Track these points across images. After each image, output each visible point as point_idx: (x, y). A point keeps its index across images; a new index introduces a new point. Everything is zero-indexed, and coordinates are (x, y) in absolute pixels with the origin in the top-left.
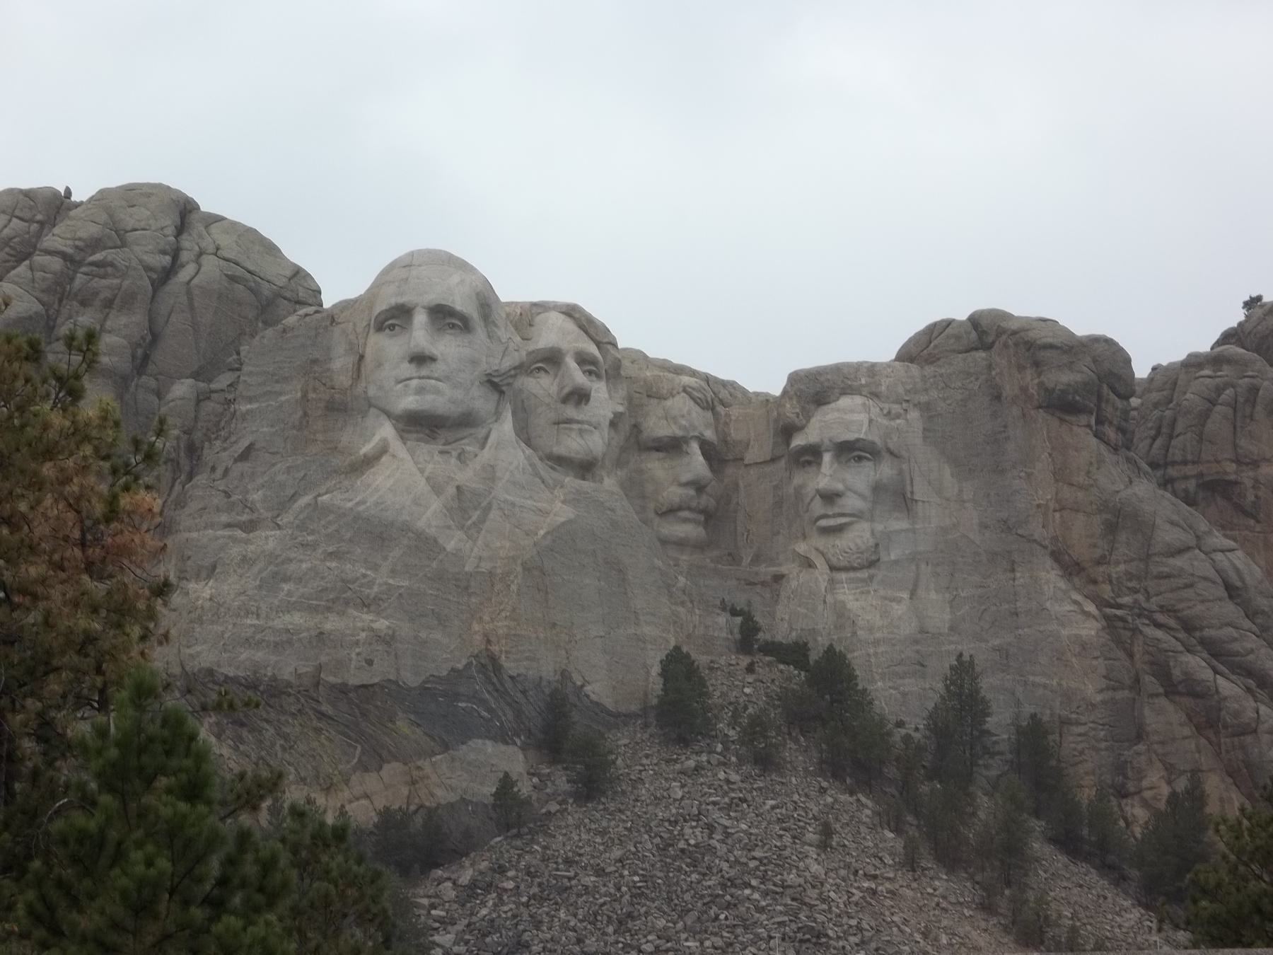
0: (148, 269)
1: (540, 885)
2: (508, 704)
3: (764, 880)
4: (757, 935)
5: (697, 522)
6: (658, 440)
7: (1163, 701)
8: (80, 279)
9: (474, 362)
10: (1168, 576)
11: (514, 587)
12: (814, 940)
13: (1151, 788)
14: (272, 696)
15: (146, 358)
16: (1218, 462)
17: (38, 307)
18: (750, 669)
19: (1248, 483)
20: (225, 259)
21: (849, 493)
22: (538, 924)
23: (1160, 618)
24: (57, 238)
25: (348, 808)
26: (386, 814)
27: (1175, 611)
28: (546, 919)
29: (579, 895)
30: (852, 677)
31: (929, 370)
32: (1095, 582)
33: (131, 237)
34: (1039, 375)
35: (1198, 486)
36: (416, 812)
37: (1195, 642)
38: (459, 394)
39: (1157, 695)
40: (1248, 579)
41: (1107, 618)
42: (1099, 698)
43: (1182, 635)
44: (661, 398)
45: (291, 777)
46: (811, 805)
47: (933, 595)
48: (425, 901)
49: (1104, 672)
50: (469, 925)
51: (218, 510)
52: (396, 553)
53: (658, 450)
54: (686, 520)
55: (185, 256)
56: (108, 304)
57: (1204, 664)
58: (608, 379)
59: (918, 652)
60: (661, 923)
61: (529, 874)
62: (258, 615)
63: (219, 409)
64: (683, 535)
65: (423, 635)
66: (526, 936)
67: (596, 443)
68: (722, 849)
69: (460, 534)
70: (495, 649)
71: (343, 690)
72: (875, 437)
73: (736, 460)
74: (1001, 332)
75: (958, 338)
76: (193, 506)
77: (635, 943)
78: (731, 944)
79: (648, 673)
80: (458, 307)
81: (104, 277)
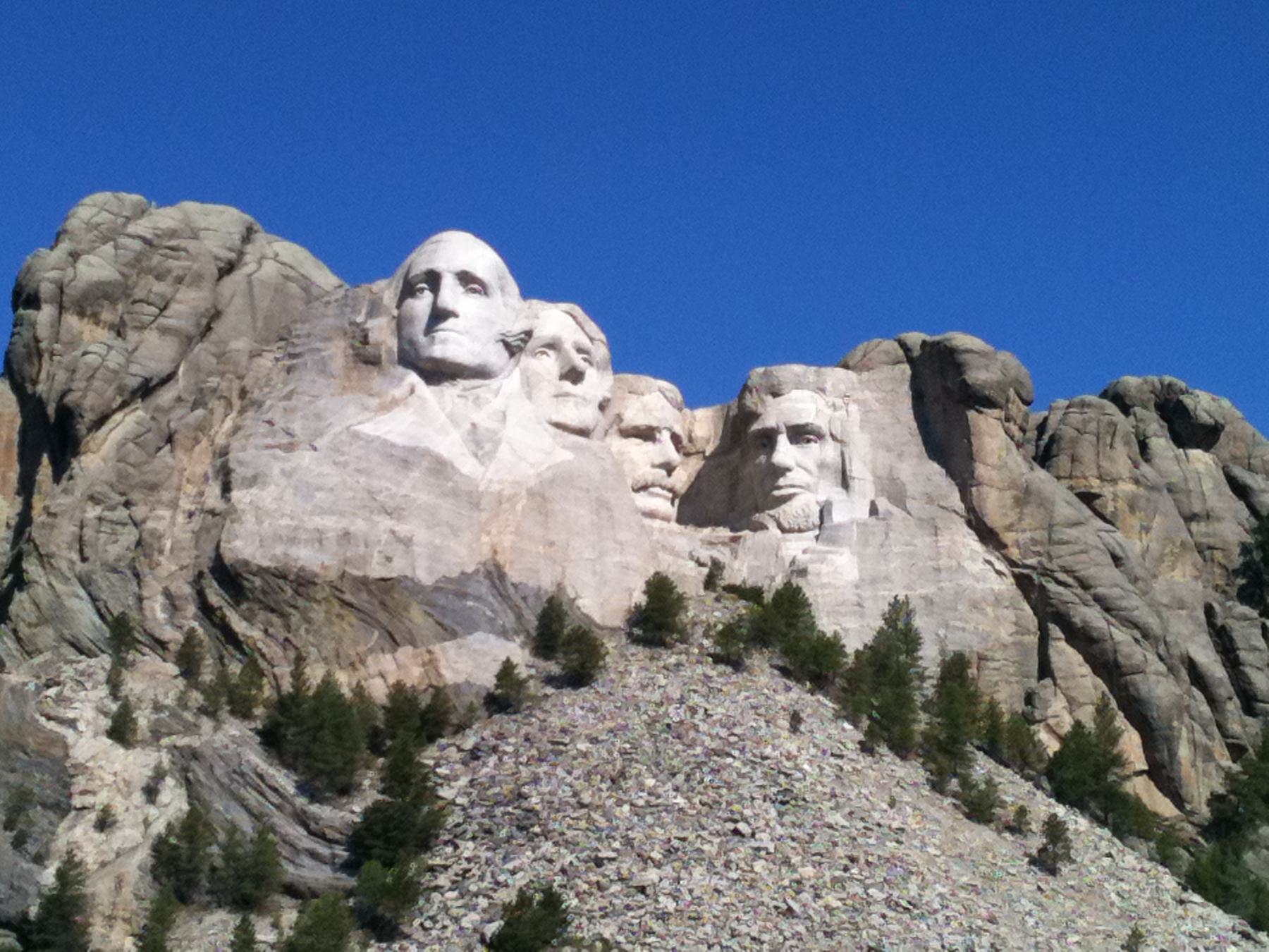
0: (217, 258)
1: (538, 749)
2: (511, 608)
3: (742, 751)
4: (742, 798)
5: (666, 498)
6: (636, 428)
7: (1063, 645)
8: (156, 260)
9: (492, 323)
10: (1067, 543)
11: (519, 507)
12: (793, 802)
13: (1056, 716)
14: (300, 585)
15: (208, 328)
16: (1086, 478)
17: (118, 276)
18: (717, 600)
19: (1110, 497)
20: (283, 264)
21: (796, 469)
22: (536, 780)
23: (1062, 576)
24: (142, 227)
25: (363, 683)
26: (398, 688)
27: (1073, 572)
28: (542, 775)
29: (575, 758)
30: (805, 604)
31: (865, 375)
32: (1005, 546)
33: (202, 234)
34: (961, 373)
36: (425, 690)
37: (1089, 597)
38: (477, 347)
39: (1059, 639)
40: (1130, 554)
41: (1015, 576)
42: (1010, 640)
43: (1079, 591)
45: (312, 657)
46: (778, 697)
47: (870, 550)
48: (431, 763)
49: (1014, 619)
50: (471, 781)
51: (265, 436)
52: (416, 474)
53: (636, 436)
54: (658, 495)
55: (248, 258)
56: (180, 280)
57: (1099, 615)
58: (598, 369)
59: (859, 596)
60: (650, 782)
61: (527, 739)
62: (292, 518)
63: (270, 364)
64: (654, 508)
65: (437, 541)
66: (525, 790)
68: (703, 727)
69: (474, 460)
70: (501, 559)
71: (364, 582)
73: (698, 453)
74: (924, 343)
75: (887, 353)
76: (240, 433)
77: (626, 798)
78: (716, 802)
79: (631, 595)
81: (177, 259)
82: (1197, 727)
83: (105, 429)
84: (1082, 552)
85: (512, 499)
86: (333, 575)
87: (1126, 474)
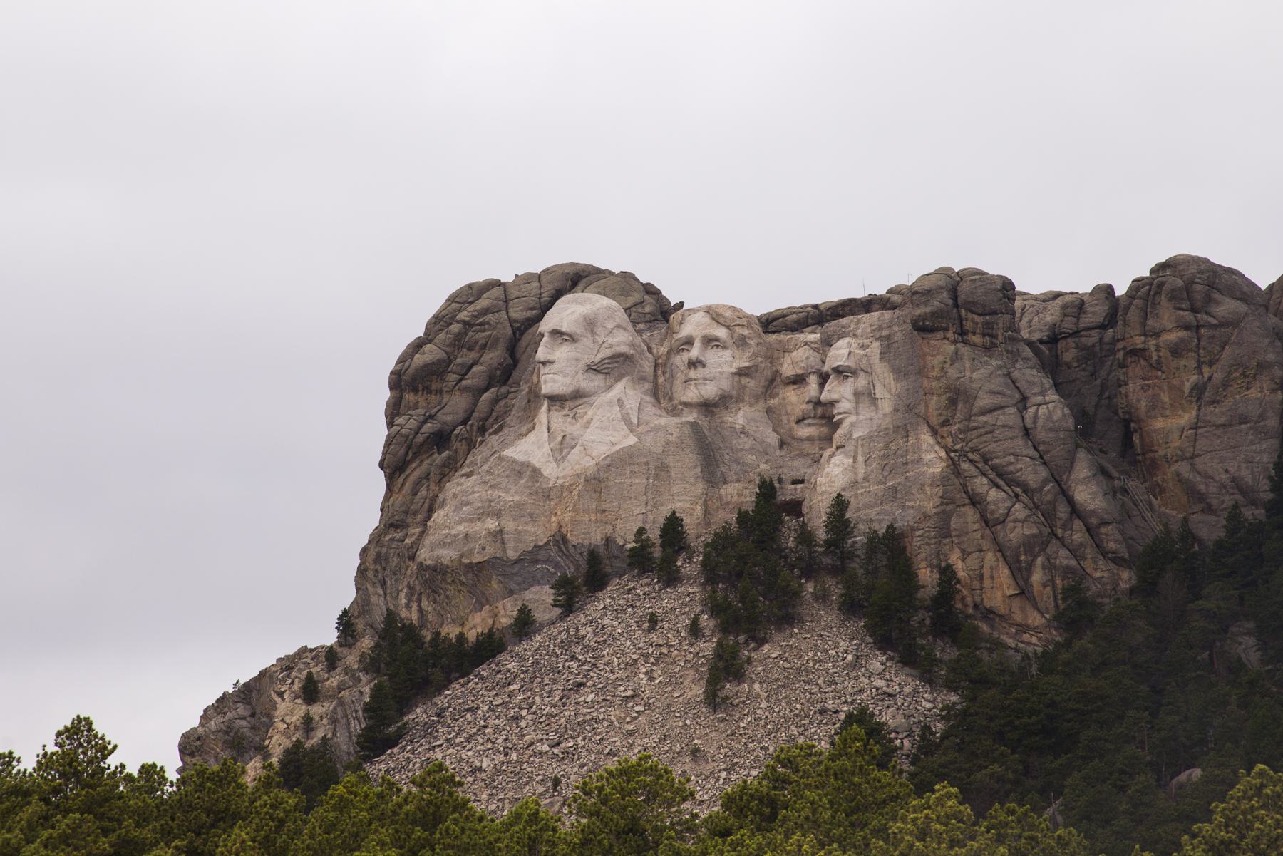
5: (822, 425)
11: (576, 492)
19: (1153, 348)
35: (1125, 355)
38: (567, 380)
39: (964, 505)
42: (934, 511)
44: (790, 352)
53: (794, 383)
54: (809, 425)
56: (484, 347)
67: (710, 391)
71: (470, 566)
72: (851, 363)
80: (564, 330)
81: (483, 331)
82: (1064, 552)
83: (403, 476)
84: (987, 433)
85: (569, 489)
86: (455, 564)
87: (1170, 325)
